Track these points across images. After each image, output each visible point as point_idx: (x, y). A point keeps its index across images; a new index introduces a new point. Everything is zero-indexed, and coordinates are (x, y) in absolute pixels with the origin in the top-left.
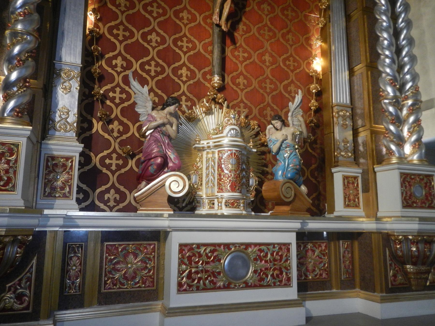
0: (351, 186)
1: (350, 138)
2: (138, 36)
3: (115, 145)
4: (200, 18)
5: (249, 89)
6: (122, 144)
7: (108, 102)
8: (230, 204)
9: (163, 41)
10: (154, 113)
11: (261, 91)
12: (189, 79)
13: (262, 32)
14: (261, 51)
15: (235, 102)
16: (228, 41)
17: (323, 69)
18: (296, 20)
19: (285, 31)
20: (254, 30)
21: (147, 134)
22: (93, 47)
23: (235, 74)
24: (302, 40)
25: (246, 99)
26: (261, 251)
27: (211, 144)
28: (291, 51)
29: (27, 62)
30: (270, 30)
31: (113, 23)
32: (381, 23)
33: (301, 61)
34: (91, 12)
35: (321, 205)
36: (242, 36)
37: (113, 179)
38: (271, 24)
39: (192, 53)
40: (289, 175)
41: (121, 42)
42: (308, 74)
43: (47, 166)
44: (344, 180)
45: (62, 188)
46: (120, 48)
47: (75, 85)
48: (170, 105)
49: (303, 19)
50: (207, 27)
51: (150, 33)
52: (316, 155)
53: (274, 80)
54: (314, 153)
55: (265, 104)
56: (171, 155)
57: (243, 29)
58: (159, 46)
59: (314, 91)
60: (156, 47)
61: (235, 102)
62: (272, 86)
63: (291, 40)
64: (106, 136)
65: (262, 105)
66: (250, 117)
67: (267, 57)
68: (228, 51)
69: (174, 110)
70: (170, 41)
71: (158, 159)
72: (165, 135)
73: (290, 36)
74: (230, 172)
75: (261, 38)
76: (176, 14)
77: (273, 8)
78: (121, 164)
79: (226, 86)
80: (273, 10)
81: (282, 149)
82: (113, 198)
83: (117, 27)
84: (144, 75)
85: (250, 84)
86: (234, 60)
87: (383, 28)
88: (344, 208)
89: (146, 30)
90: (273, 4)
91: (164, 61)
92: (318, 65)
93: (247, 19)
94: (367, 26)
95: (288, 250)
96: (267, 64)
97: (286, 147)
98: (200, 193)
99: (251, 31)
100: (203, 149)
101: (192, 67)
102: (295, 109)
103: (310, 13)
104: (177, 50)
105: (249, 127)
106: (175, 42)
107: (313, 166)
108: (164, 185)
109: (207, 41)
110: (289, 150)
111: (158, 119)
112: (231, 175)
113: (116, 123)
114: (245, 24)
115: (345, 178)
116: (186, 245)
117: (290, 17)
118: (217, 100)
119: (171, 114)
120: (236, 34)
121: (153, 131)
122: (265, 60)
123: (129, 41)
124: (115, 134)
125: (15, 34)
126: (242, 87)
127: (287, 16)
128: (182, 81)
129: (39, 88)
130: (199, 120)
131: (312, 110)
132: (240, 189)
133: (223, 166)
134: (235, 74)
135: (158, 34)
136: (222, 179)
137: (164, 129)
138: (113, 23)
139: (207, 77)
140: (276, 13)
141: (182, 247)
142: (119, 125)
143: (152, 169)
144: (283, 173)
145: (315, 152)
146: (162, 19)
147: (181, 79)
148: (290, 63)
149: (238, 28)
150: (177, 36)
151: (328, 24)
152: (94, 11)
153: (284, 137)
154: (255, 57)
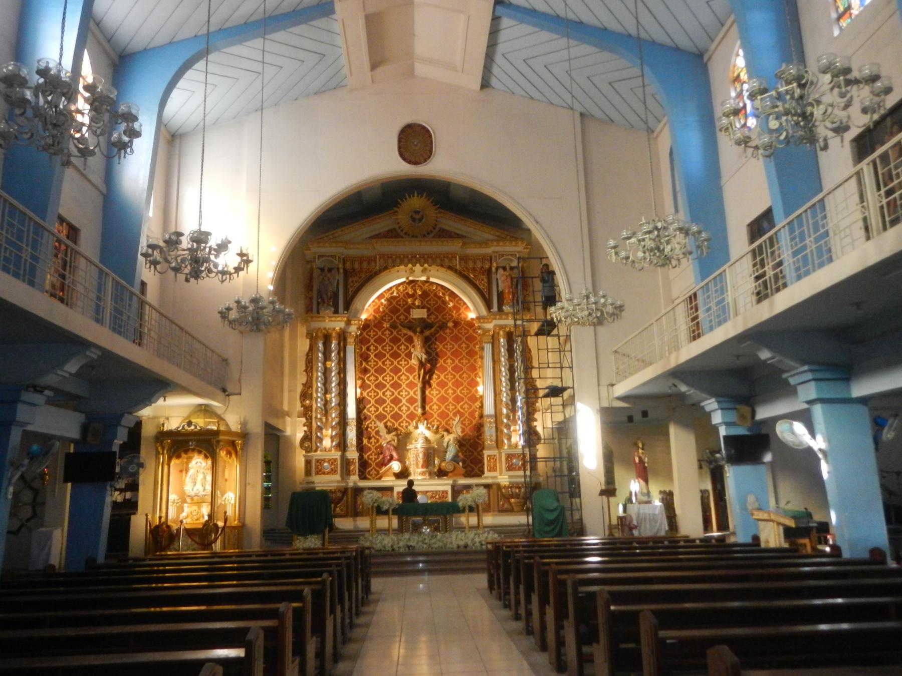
1: (494, 435)
2: (381, 394)
3: (373, 449)
6: (376, 449)
8: (423, 473)
9: (393, 394)
10: (387, 436)
16: (427, 386)
20: (442, 377)
24: (473, 376)
47: (354, 429)
56: (395, 455)
67: (450, 391)
68: (427, 392)
70: (396, 393)
73: (465, 375)
77: (454, 361)
80: (454, 361)
85: (440, 407)
92: (480, 389)
106: (399, 393)
125: (333, 419)
143: (386, 461)
152: (360, 387)
154: (443, 392)
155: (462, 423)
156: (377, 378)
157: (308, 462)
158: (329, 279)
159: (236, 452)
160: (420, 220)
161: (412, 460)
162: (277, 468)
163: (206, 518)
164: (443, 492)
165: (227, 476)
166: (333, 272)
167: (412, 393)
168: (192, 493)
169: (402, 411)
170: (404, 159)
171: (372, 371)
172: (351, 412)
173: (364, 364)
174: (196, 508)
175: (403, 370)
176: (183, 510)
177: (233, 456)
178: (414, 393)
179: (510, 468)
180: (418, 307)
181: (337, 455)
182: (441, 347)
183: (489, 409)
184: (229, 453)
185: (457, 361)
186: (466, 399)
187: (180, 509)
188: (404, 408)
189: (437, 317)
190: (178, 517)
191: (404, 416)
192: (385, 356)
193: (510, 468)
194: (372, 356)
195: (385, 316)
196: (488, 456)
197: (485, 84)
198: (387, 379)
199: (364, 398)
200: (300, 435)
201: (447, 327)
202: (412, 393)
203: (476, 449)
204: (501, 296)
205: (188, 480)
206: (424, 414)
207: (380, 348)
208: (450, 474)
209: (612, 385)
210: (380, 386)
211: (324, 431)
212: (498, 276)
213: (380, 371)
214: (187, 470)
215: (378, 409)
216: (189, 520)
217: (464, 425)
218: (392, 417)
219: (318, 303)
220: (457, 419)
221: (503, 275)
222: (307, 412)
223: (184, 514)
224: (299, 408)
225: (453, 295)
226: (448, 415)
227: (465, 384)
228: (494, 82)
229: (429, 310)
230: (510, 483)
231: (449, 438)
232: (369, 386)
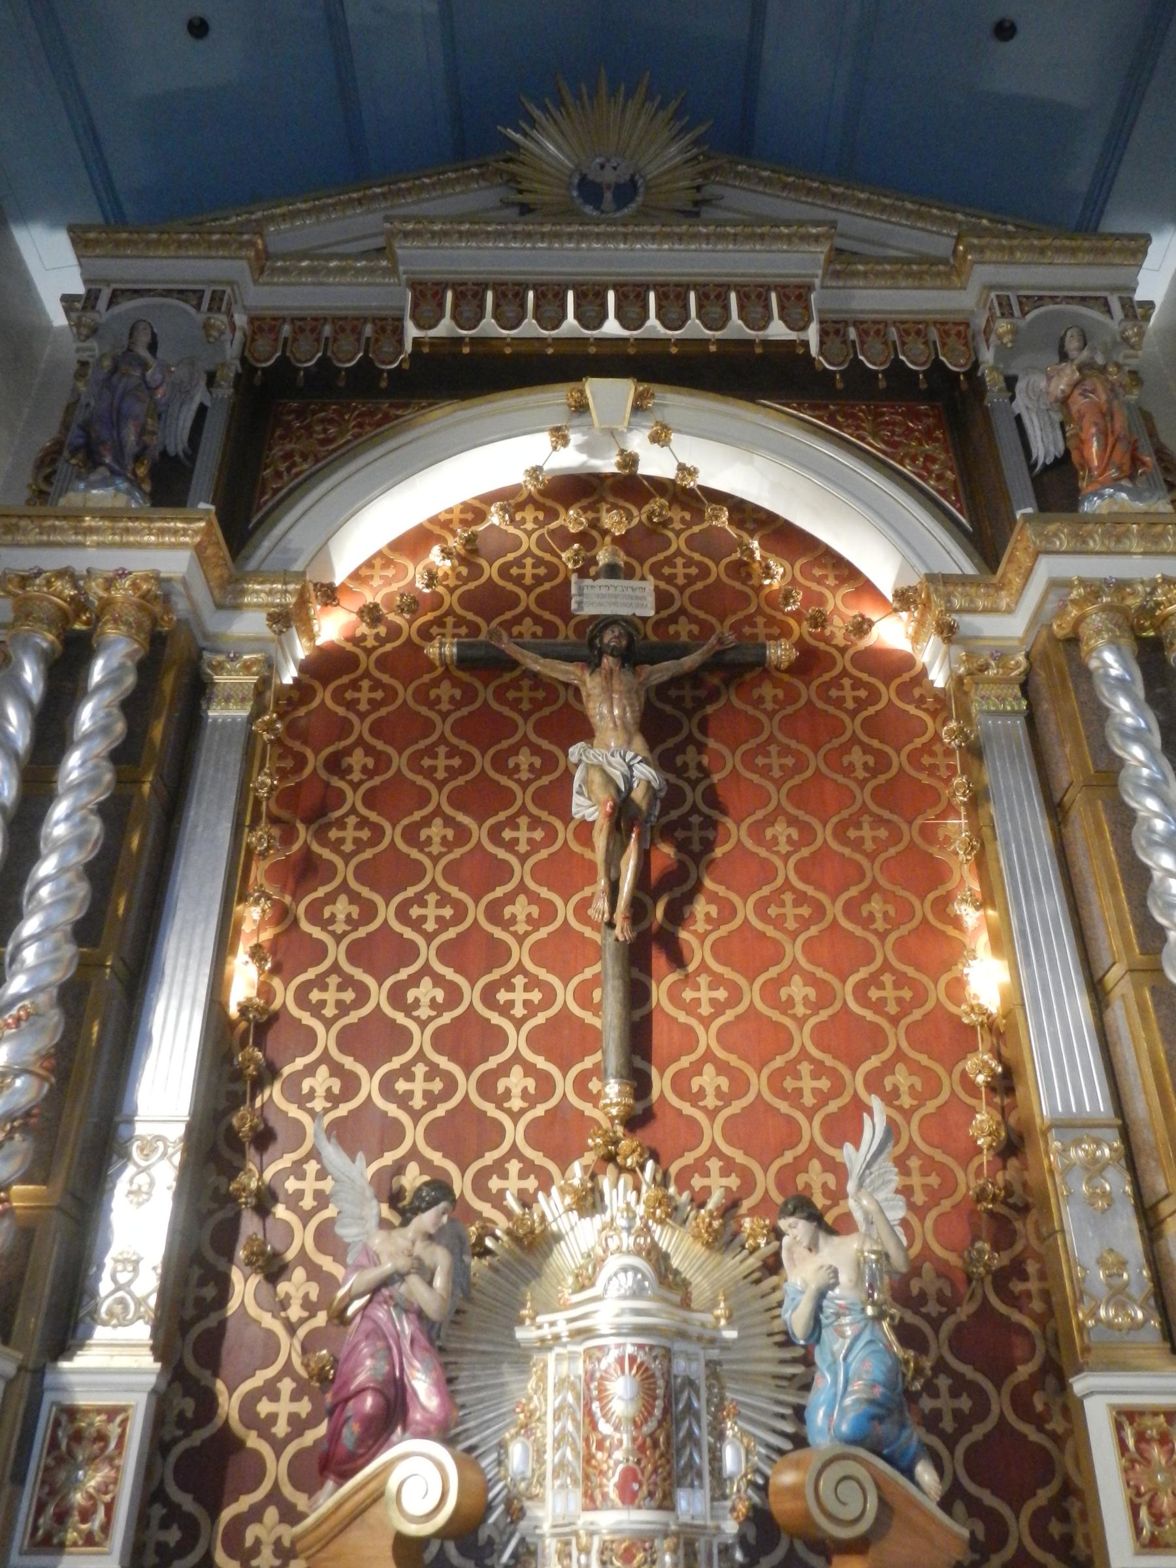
0: (1156, 1452)
2: (379, 996)
4: (565, 911)
5: (737, 1107)
7: (280, 1211)
9: (454, 995)
10: (377, 1240)
11: (783, 1107)
12: (531, 1100)
13: (773, 911)
14: (773, 972)
15: (689, 1158)
16: (659, 960)
17: (1004, 998)
18: (892, 851)
19: (854, 891)
20: (746, 910)
21: (350, 1311)
22: (237, 1057)
23: (685, 1062)
25: (730, 1142)
27: (563, 1329)
28: (885, 951)
29: (7, 1144)
30: (801, 899)
32: (1147, 820)
33: (925, 980)
34: (247, 958)
35: (1079, 1541)
36: (702, 938)
37: (277, 1469)
38: (805, 879)
39: (540, 1018)
40: (844, 1428)
41: (328, 1023)
42: (955, 1020)
43: (54, 1444)
44: (1119, 1427)
45: (86, 1516)
48: (424, 1210)
49: (918, 840)
50: (588, 932)
51: (414, 980)
52: (1028, 1323)
53: (829, 1061)
54: (1016, 1316)
55: (801, 1148)
57: (707, 914)
58: (439, 1015)
59: (981, 1079)
60: (431, 1019)
61: (689, 1158)
62: (824, 1084)
63: (879, 916)
65: (788, 1157)
66: (746, 1204)
67: (797, 989)
68: (659, 993)
69: (435, 1224)
70: (472, 995)
71: (365, 1401)
72: (406, 1311)
73: (876, 905)
74: (617, 1428)
75: (770, 931)
76: (494, 913)
78: (304, 1415)
79: (656, 1109)
80: (807, 833)
81: (824, 1321)
82: (273, 1538)
83: (320, 983)
85: (739, 1085)
86: (682, 1017)
87: (1156, 838)
88: (1137, 1554)
89: (403, 974)
90: (807, 818)
91: (453, 1058)
92: (986, 980)
93: (714, 880)
94: (1113, 834)
96: (800, 1010)
97: (838, 1315)
98: (540, 1513)
99: (734, 912)
100: (544, 1345)
101: (541, 1062)
102: (869, 1166)
103: (943, 815)
105: (737, 1241)
107: (1024, 1372)
108: (382, 1494)
109: (589, 973)
110: (851, 1324)
111: (383, 1258)
112: (621, 1441)
113: (299, 1274)
114: (713, 898)
115: (1125, 1417)
117: (869, 846)
118: (619, 1159)
119: (430, 1237)
120: (683, 935)
121: (370, 1301)
122: (790, 999)
123: (353, 1017)
124: (295, 1312)
126: (711, 1102)
127: (858, 844)
128: (509, 1112)
129: (50, 1207)
130: (557, 1238)
131: (979, 1150)
132: (659, 1495)
133: (596, 1406)
134: (685, 1062)
135: (438, 980)
136: (593, 1457)
137: (401, 1289)
138: (311, 974)
139: (591, 1086)
140: (819, 842)
142: (308, 1280)
143: (350, 1433)
144: (829, 1415)
145: (1021, 1311)
146: (451, 933)
147: (506, 1105)
148: (882, 994)
149: (692, 914)
150: (496, 974)
151: (989, 847)
152: (257, 953)
153: (823, 1278)
154: (753, 995)
155: (901, 1163)
156: (368, 912)
161: (550, 1430)
167: (565, 996)
169: (500, 1101)
171: (345, 872)
173: (303, 833)
175: (522, 872)
178: (583, 996)
180: (612, 571)
182: (733, 761)
183: (1065, 1080)
186: (897, 1038)
191: (515, 1134)
192: (423, 798)
194: (353, 798)
195: (440, 622)
196: (1125, 1417)
198: (428, 918)
199: (274, 1017)
201: (759, 665)
202: (565, 996)
203: (999, 1371)
206: (638, 1119)
207: (399, 762)
210: (381, 953)
212: (1020, 405)
213: (390, 874)
215: (350, 1084)
218: (438, 1135)
226: (793, 1134)
227: (885, 951)
231: (819, 1268)
232: (321, 951)
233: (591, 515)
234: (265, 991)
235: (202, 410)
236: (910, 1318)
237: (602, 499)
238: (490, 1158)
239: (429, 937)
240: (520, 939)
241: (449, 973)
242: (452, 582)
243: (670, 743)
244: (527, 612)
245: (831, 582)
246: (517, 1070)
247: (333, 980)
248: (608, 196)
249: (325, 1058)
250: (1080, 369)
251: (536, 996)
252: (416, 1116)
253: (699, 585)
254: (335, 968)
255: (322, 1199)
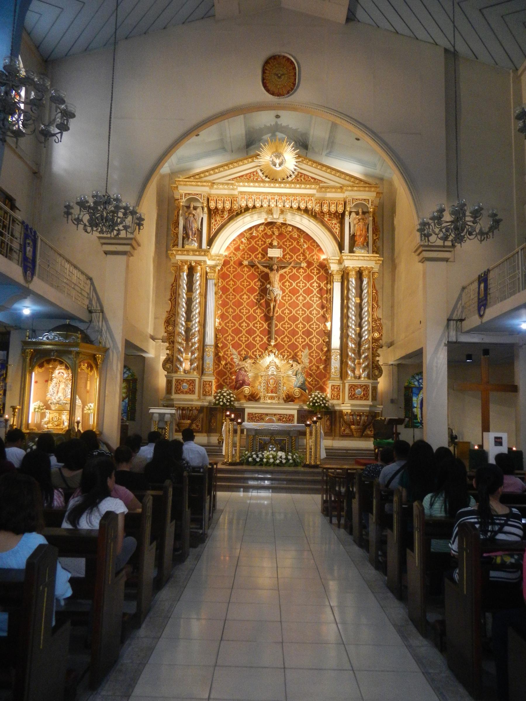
7: (225, 356)
9: (248, 325)
26: (281, 417)
31: (227, 321)
39: (262, 329)
43: (204, 385)
46: (230, 331)
51: (242, 322)
64: (225, 370)
67: (300, 325)
70: (251, 325)
84: (240, 342)
89: (241, 321)
91: (248, 334)
95: (293, 417)
101: (262, 336)
104: (255, 329)
116: (250, 413)
117: (315, 301)
124: (228, 369)
126: (286, 342)
135: (246, 323)
141: (249, 414)
150: (255, 322)
156: (235, 311)
157: (169, 382)
158: (194, 215)
159: (97, 365)
160: (280, 165)
162: (142, 388)
163: (66, 424)
164: (290, 415)
165: (88, 388)
166: (198, 210)
168: (55, 401)
169: (256, 341)
170: (268, 91)
172: (210, 339)
174: (57, 415)
176: (45, 417)
177: (94, 369)
179: (352, 397)
181: (195, 375)
184: (90, 367)
185: (308, 299)
187: (43, 415)
188: (258, 339)
189: (292, 257)
190: (41, 422)
191: (258, 346)
192: (242, 290)
193: (352, 397)
197: (351, 17)
200: (163, 358)
204: (353, 238)
205: (50, 388)
208: (296, 401)
209: (462, 320)
211: (184, 355)
214: (51, 379)
216: (50, 425)
217: (312, 357)
218: (248, 346)
219: (183, 238)
220: (307, 351)
221: (355, 219)
222: (170, 339)
223: (46, 419)
224: (162, 333)
225: (308, 237)
226: (297, 347)
228: (360, 14)
229: (284, 250)
230: (351, 410)
233: (272, 230)
234: (220, 324)
235: (202, 218)
236: (311, 372)
237: (274, 225)
238: (254, 350)
239: (244, 315)
240: (258, 316)
241: (248, 321)
242: (246, 245)
243: (284, 281)
244: (260, 252)
245: (315, 246)
246: (258, 337)
247: (230, 322)
248: (277, 165)
249: (230, 334)
250: (359, 220)
251: (261, 325)
252: (243, 343)
253: (291, 247)
254: (230, 320)
255: (231, 355)
